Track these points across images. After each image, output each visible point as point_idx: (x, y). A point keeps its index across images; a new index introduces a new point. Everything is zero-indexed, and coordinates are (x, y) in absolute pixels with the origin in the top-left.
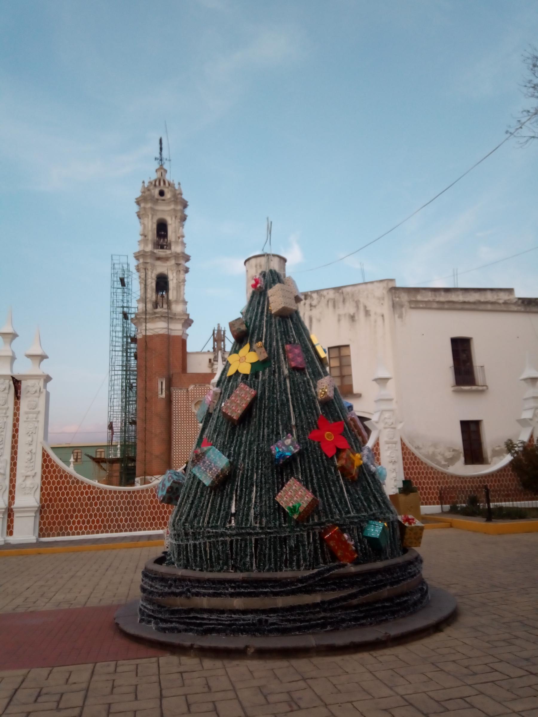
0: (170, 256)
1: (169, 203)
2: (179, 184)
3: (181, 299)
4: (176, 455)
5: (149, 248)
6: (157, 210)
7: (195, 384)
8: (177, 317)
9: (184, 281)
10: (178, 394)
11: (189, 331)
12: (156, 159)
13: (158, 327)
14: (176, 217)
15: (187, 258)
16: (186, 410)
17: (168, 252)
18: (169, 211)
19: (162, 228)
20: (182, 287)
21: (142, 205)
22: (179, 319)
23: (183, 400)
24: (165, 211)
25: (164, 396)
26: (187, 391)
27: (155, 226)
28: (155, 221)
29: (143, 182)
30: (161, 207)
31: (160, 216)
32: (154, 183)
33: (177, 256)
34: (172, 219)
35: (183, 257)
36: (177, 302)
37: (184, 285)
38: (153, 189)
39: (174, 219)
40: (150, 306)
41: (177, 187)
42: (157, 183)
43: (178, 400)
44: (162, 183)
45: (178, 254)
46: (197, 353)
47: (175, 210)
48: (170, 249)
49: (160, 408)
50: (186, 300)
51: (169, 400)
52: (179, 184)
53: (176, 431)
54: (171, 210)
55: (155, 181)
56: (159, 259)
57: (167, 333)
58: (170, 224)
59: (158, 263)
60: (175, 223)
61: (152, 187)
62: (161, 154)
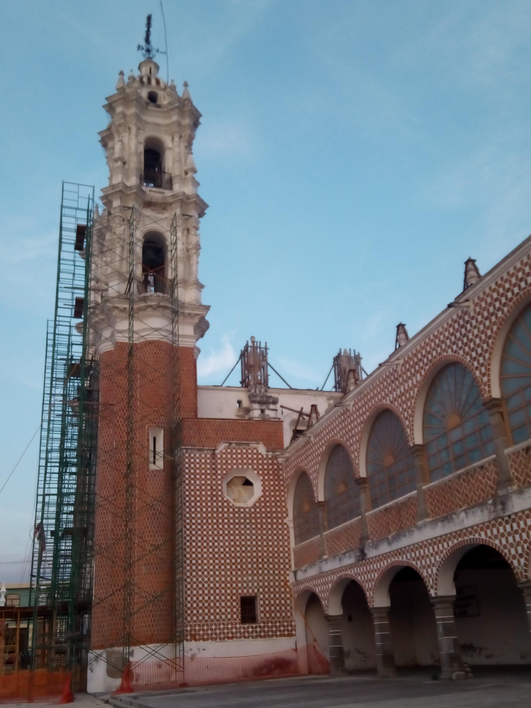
0: (170, 200)
1: (168, 113)
2: (186, 85)
3: (192, 279)
4: (192, 596)
5: (133, 181)
6: (147, 123)
7: (225, 439)
8: (187, 311)
9: (198, 247)
10: (194, 460)
11: (200, 344)
12: (139, 47)
13: (152, 327)
14: (181, 137)
15: (202, 208)
16: (212, 496)
17: (168, 193)
18: (168, 125)
19: (153, 155)
20: (194, 257)
21: (119, 109)
22: (189, 314)
23: (206, 474)
24: (160, 124)
25: (160, 464)
26: (214, 456)
27: (141, 149)
28: (142, 139)
29: (122, 73)
30: (153, 118)
31: (149, 132)
32: (138, 79)
33: (184, 201)
34: (173, 138)
35: (196, 203)
36: (185, 283)
37: (198, 255)
38: (138, 88)
39: (177, 139)
40: (134, 287)
41: (180, 91)
42: (145, 80)
43: (195, 474)
44: (153, 82)
45: (188, 198)
46: (216, 388)
47: (179, 124)
48: (171, 188)
49: (155, 488)
50: (201, 281)
51: (173, 473)
52: (186, 85)
53: (191, 541)
54: (173, 123)
55: (141, 78)
56: (149, 204)
57: (167, 339)
58: (170, 149)
59: (148, 212)
60: (179, 146)
61: (136, 84)
62: (147, 40)
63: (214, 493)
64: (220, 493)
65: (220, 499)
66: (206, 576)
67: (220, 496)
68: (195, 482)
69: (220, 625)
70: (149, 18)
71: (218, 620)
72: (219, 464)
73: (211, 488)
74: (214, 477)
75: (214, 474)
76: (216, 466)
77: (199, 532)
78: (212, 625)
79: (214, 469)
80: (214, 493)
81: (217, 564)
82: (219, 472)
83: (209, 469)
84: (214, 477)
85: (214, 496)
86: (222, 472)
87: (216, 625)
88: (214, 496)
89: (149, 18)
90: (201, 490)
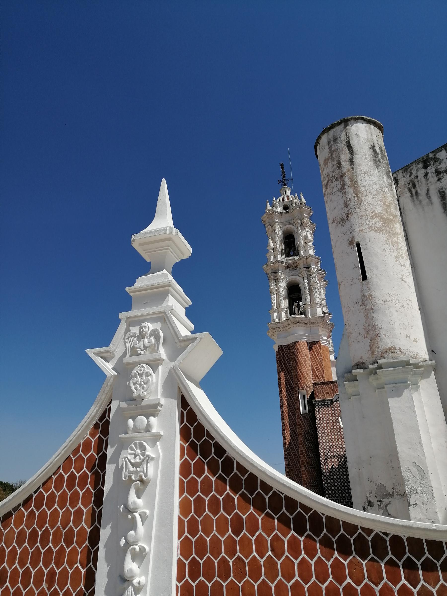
63: (335, 424)
64: (338, 424)
65: (338, 427)
66: (334, 472)
67: (338, 425)
68: (323, 419)
69: (345, 499)
70: (282, 165)
71: (344, 497)
72: (336, 407)
73: (333, 421)
74: (334, 415)
75: (333, 413)
76: (334, 409)
77: (338, 477)
78: (341, 500)
79: (333, 410)
80: (335, 424)
81: (330, 436)
82: (336, 412)
83: (330, 411)
84: (334, 415)
85: (335, 426)
86: (338, 411)
87: (343, 500)
88: (335, 426)
89: (282, 165)
90: (327, 423)
